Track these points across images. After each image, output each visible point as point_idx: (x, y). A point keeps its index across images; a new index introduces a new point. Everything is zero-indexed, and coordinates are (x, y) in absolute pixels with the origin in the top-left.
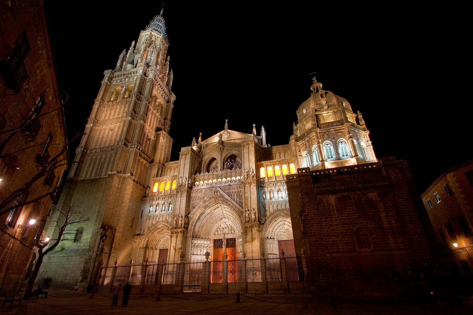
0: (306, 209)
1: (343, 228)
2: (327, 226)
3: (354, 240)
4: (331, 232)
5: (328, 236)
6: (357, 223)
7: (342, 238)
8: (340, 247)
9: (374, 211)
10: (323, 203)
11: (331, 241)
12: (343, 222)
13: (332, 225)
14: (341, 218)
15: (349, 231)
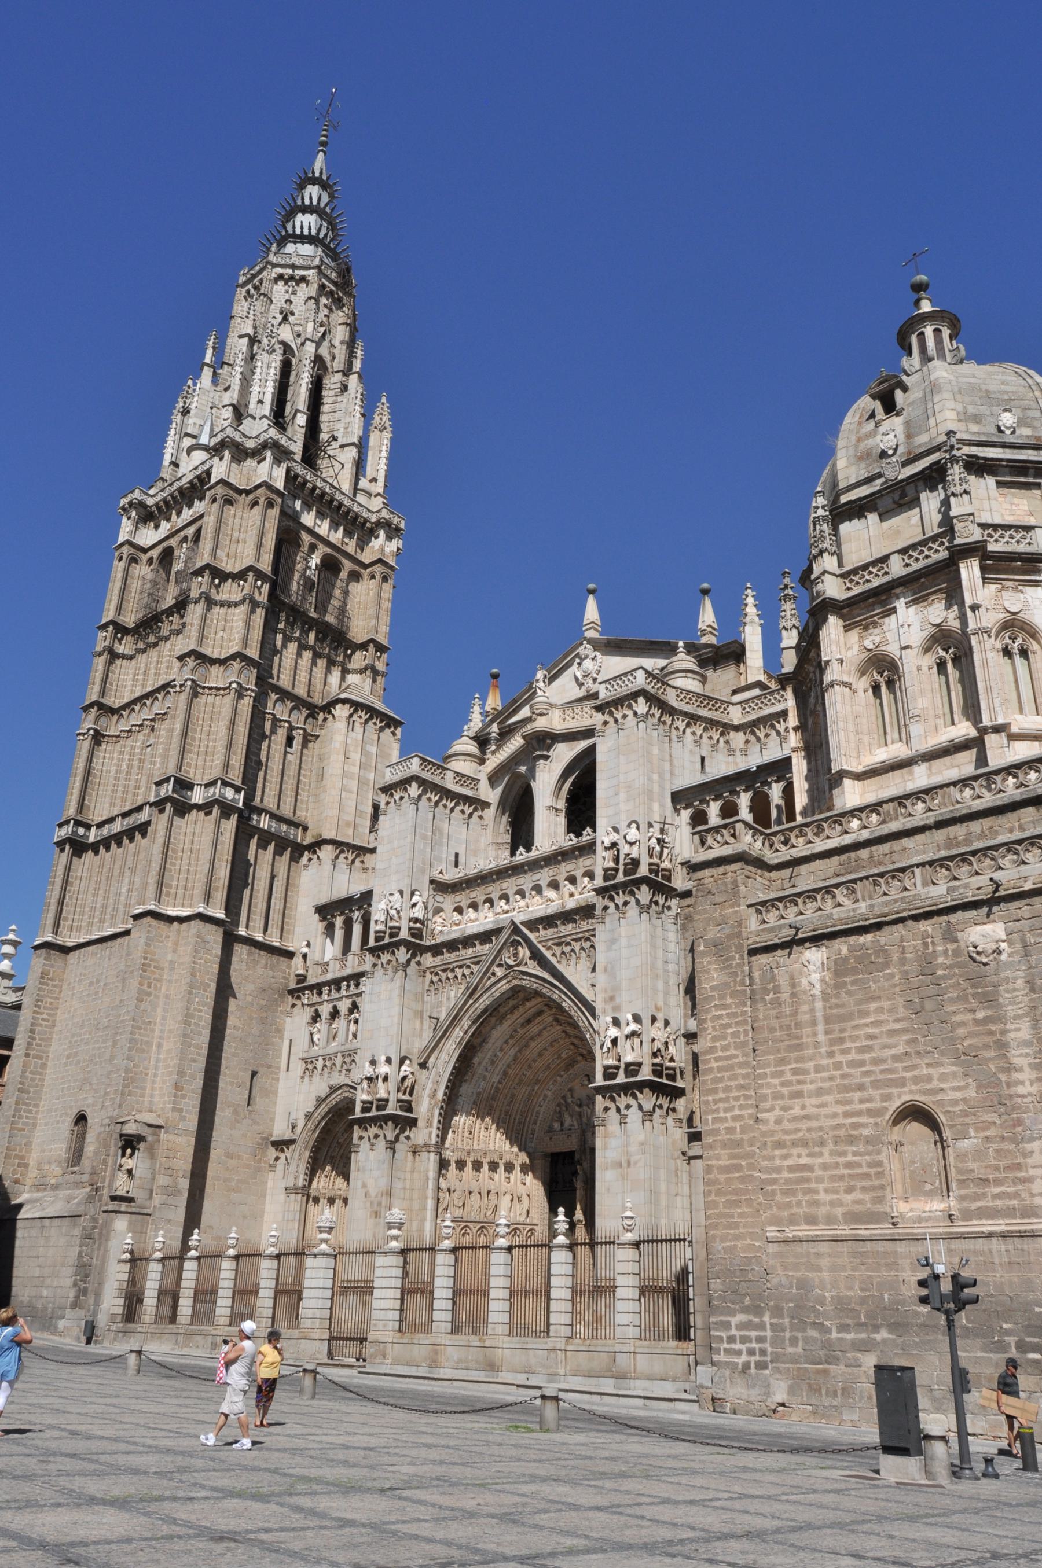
0: (709, 1024)
1: (840, 1109)
2: (781, 1097)
3: (880, 1164)
4: (792, 1126)
5: (779, 1145)
6: (901, 1083)
7: (831, 1154)
8: (822, 1196)
9: (980, 1015)
10: (777, 990)
11: (791, 1169)
12: (843, 1076)
13: (799, 1095)
14: (839, 1058)
15: (864, 1120)
